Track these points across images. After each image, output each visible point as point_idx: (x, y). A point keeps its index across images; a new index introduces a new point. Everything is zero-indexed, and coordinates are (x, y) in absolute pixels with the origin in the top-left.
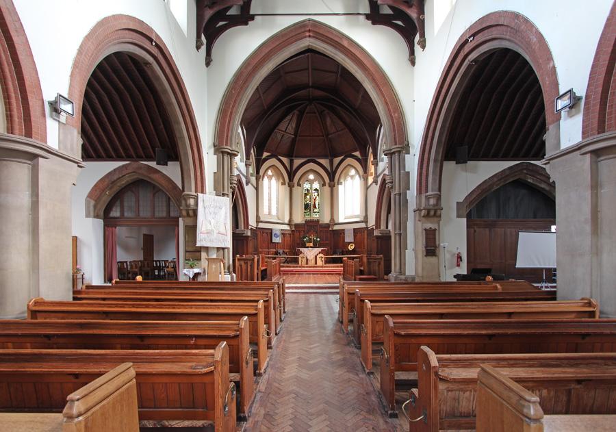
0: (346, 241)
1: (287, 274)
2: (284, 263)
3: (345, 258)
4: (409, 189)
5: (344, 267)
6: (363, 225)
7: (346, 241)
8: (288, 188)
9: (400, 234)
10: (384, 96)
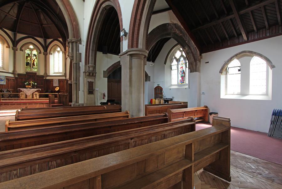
0: (54, 86)
1: (8, 104)
2: (8, 97)
3: (50, 94)
4: (81, 62)
5: (49, 99)
6: (64, 78)
7: (54, 86)
8: (12, 51)
9: (76, 83)
10: (68, 11)
